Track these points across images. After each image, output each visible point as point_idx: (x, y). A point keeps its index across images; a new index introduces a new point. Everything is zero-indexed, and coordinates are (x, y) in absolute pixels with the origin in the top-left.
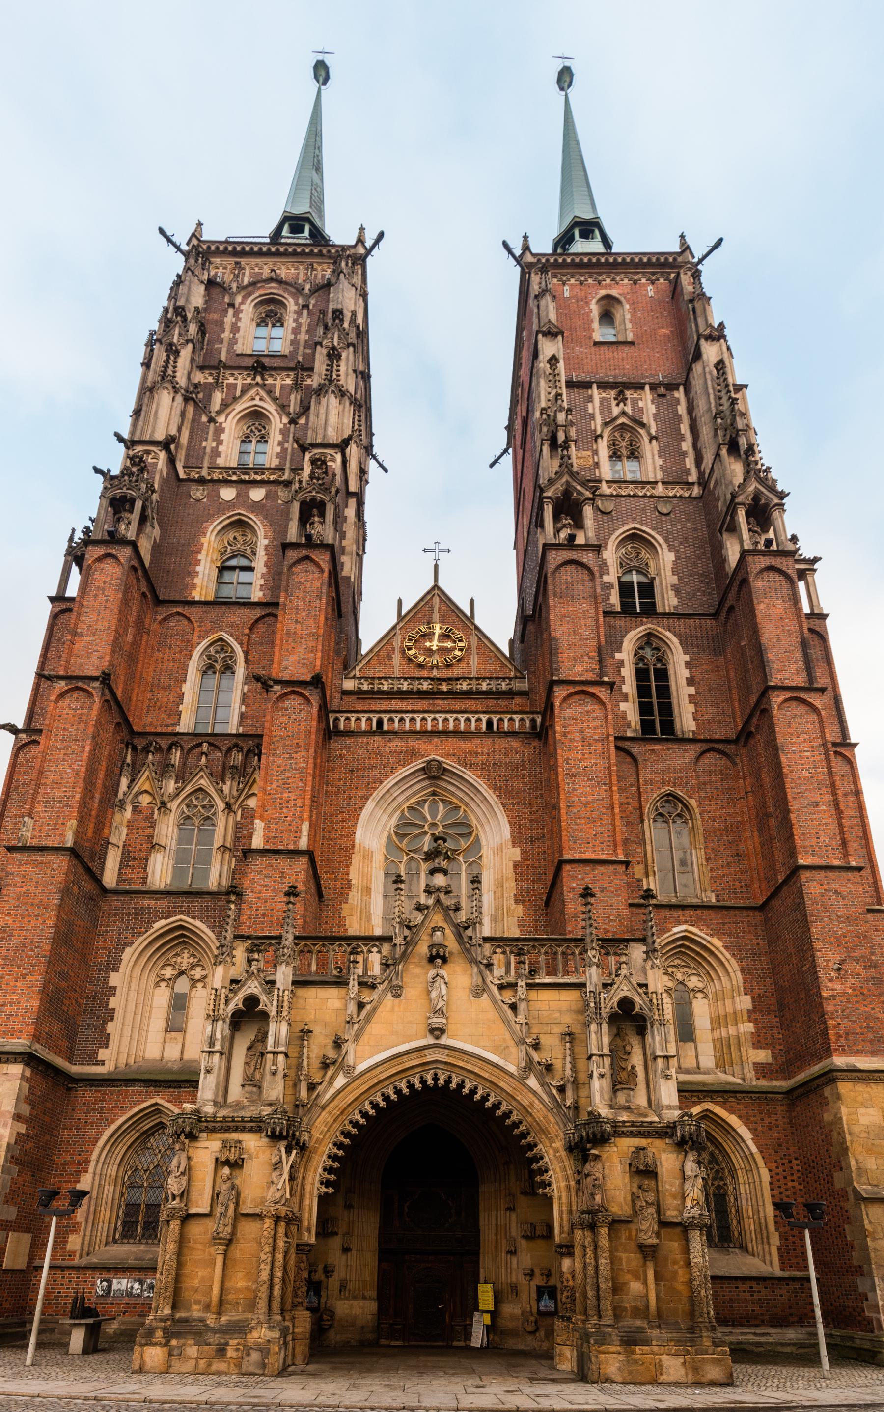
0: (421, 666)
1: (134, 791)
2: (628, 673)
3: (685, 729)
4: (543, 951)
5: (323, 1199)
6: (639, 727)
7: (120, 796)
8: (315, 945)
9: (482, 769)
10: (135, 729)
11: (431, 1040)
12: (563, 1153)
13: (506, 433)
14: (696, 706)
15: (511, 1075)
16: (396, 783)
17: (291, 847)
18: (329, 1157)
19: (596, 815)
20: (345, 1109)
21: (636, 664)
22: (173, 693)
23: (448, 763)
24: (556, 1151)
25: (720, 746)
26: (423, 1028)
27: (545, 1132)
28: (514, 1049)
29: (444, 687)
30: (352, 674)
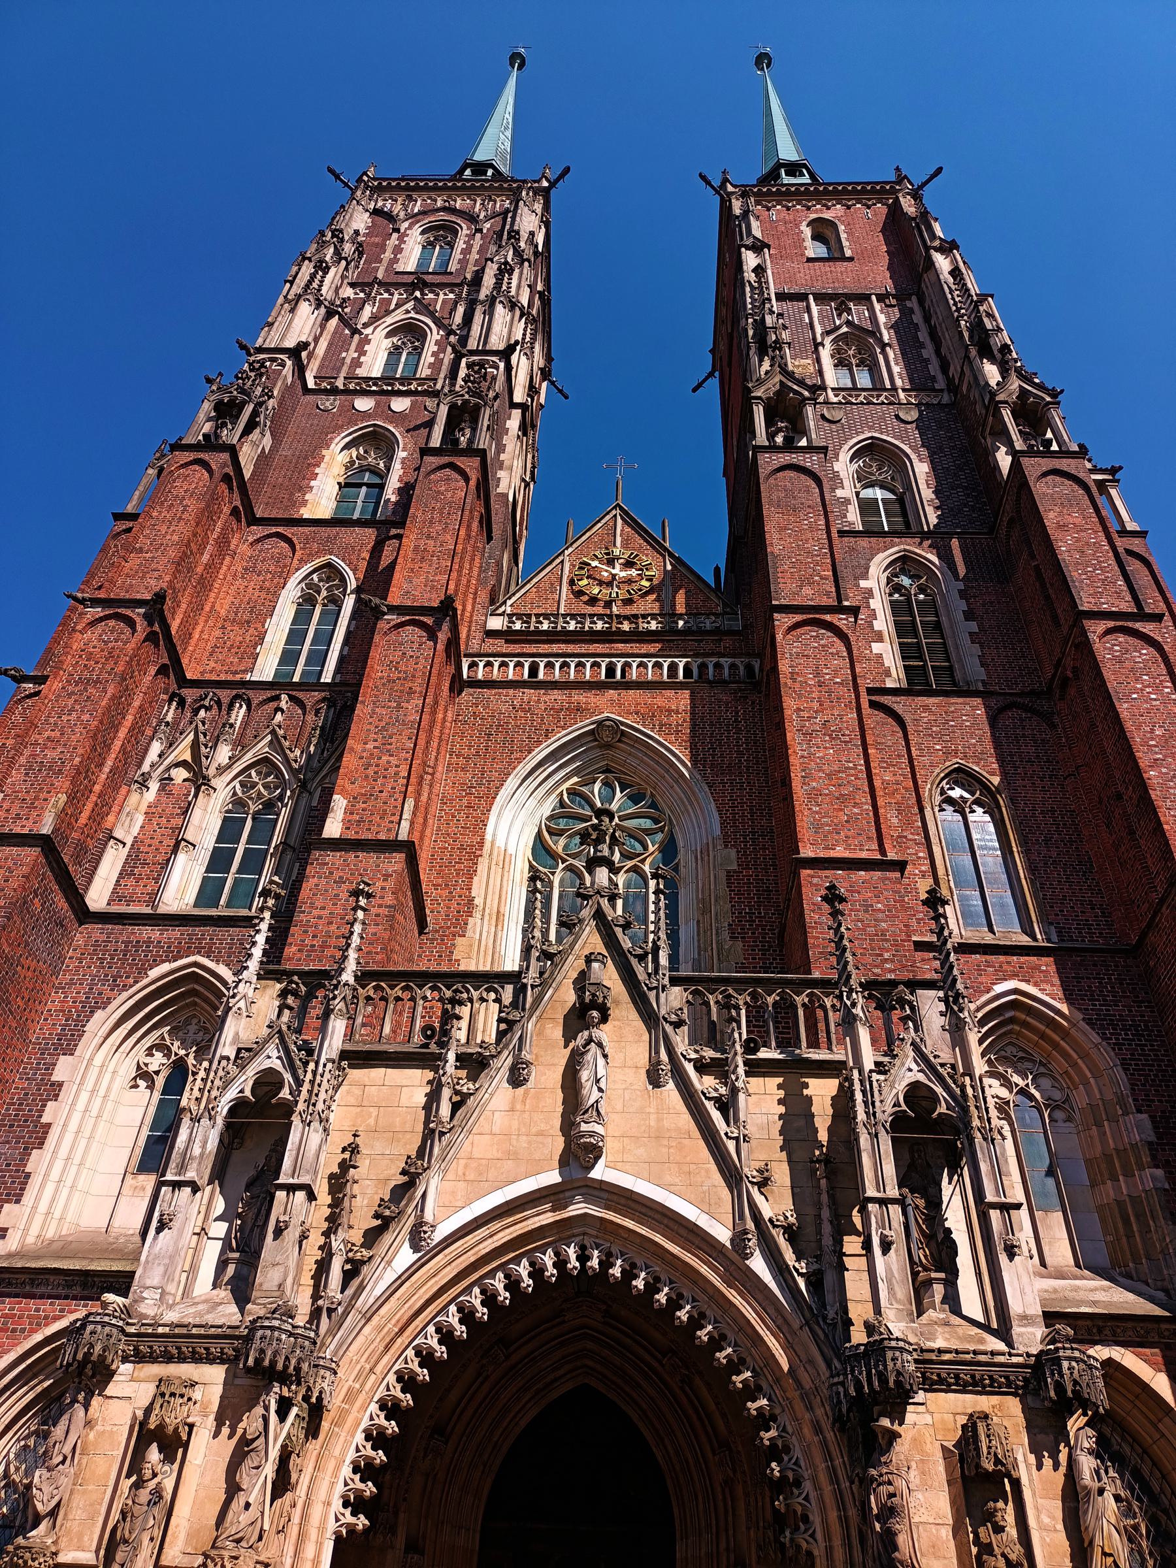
0: (593, 601)
1: (167, 762)
2: (879, 604)
6: (902, 675)
7: (146, 767)
8: (392, 987)
9: (677, 732)
10: (189, 676)
13: (710, 356)
14: (982, 647)
17: (382, 836)
21: (891, 595)
22: (252, 631)
24: (818, 1429)
29: (626, 626)
30: (501, 610)
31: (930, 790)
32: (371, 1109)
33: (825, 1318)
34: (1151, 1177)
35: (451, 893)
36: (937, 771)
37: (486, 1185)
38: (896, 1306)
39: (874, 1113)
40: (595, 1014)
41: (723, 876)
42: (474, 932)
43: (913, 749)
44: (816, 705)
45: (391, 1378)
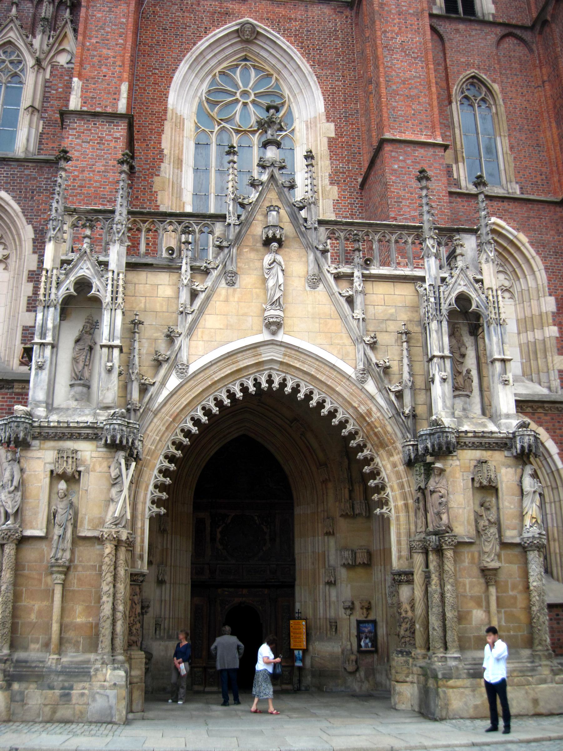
3: (486, 12)
4: (377, 238)
5: (155, 520)
6: (443, 5)
9: (296, 36)
11: (265, 336)
12: (401, 468)
15: (348, 378)
16: (210, 46)
17: (109, 110)
18: (160, 471)
19: (414, 92)
20: (178, 415)
23: (262, 27)
24: (394, 465)
25: (518, 32)
26: (258, 323)
27: (382, 445)
28: (350, 349)
31: (456, 90)
32: (141, 298)
33: (403, 413)
34: (553, 331)
35: (147, 145)
36: (461, 77)
37: (216, 343)
38: (446, 410)
39: (440, 310)
40: (275, 244)
41: (325, 141)
42: (165, 173)
43: (448, 60)
44: (396, 29)
45: (170, 444)
